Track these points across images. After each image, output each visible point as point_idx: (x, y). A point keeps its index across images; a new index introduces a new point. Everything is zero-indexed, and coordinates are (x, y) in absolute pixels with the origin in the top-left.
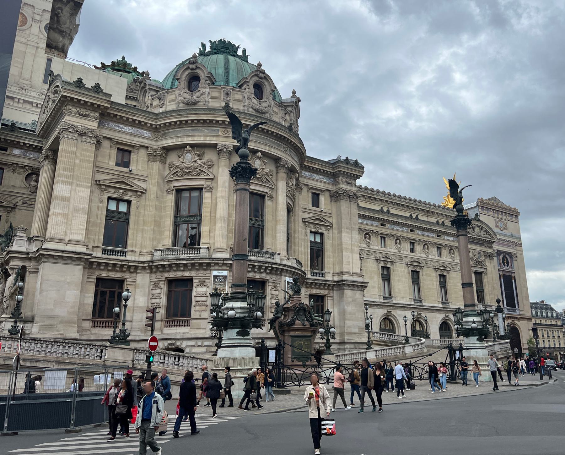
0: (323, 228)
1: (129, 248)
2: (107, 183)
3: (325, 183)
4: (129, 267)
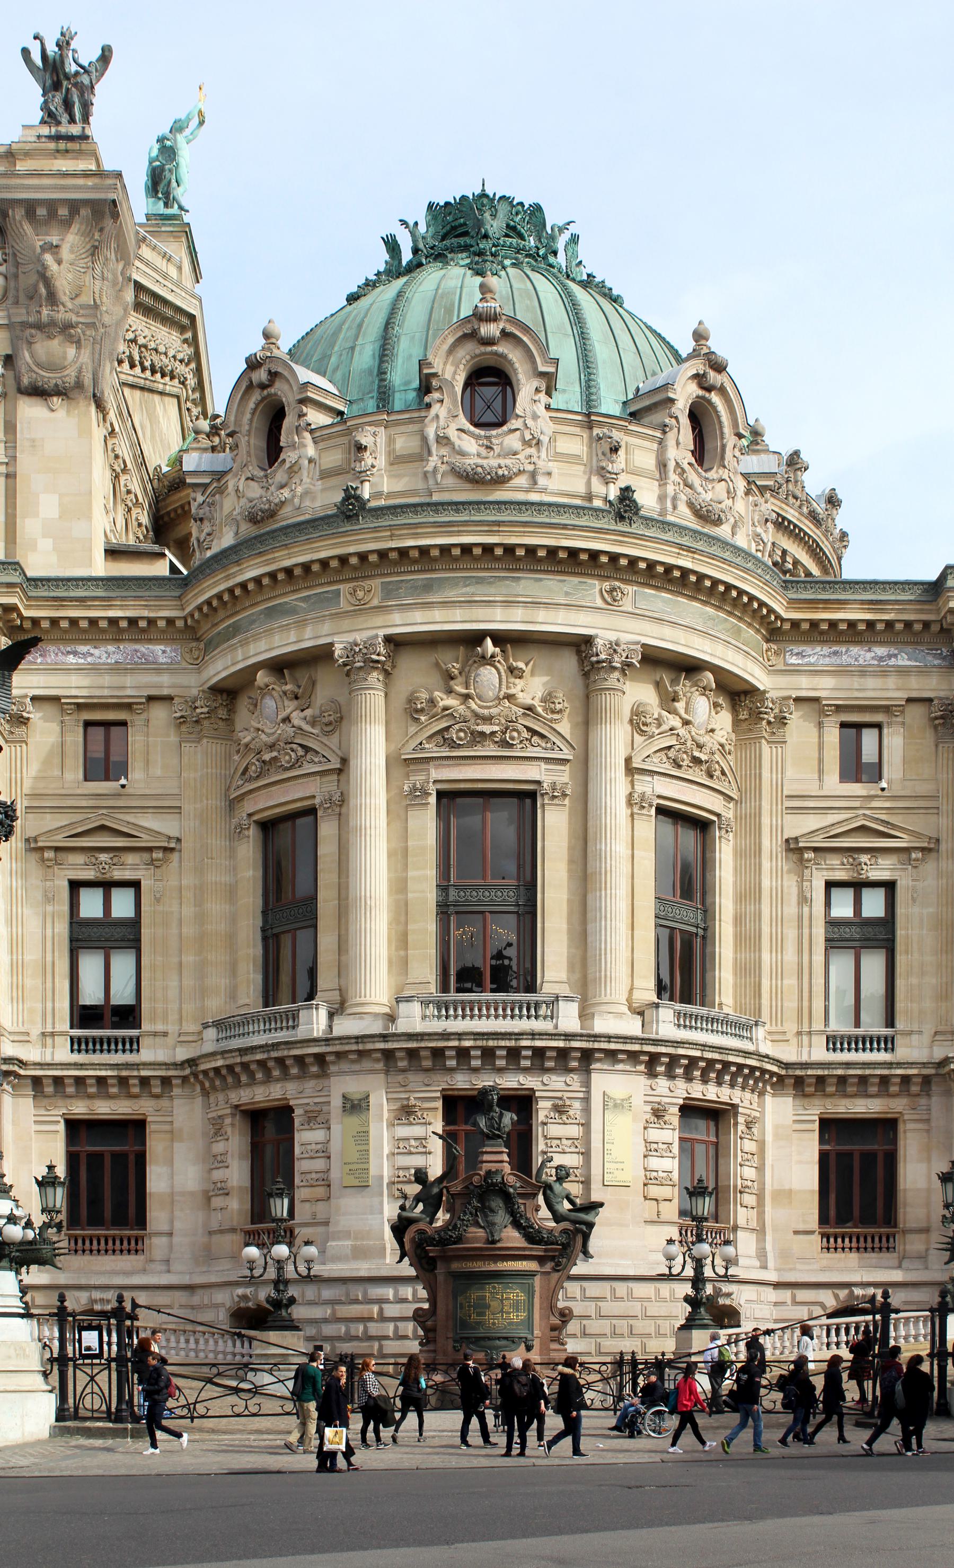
4: (145, 1082)
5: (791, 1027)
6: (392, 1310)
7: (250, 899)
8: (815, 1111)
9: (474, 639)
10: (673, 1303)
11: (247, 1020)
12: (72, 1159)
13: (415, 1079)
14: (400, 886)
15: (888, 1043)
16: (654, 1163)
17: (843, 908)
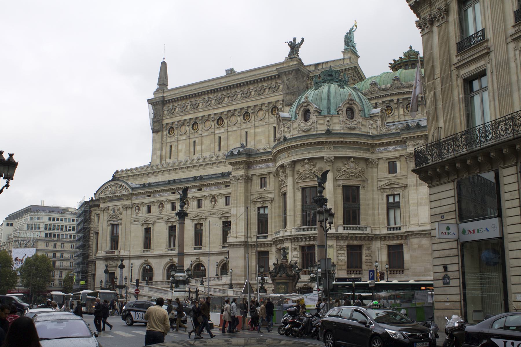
0: (398, 189)
1: (269, 233)
2: (255, 200)
3: (399, 150)
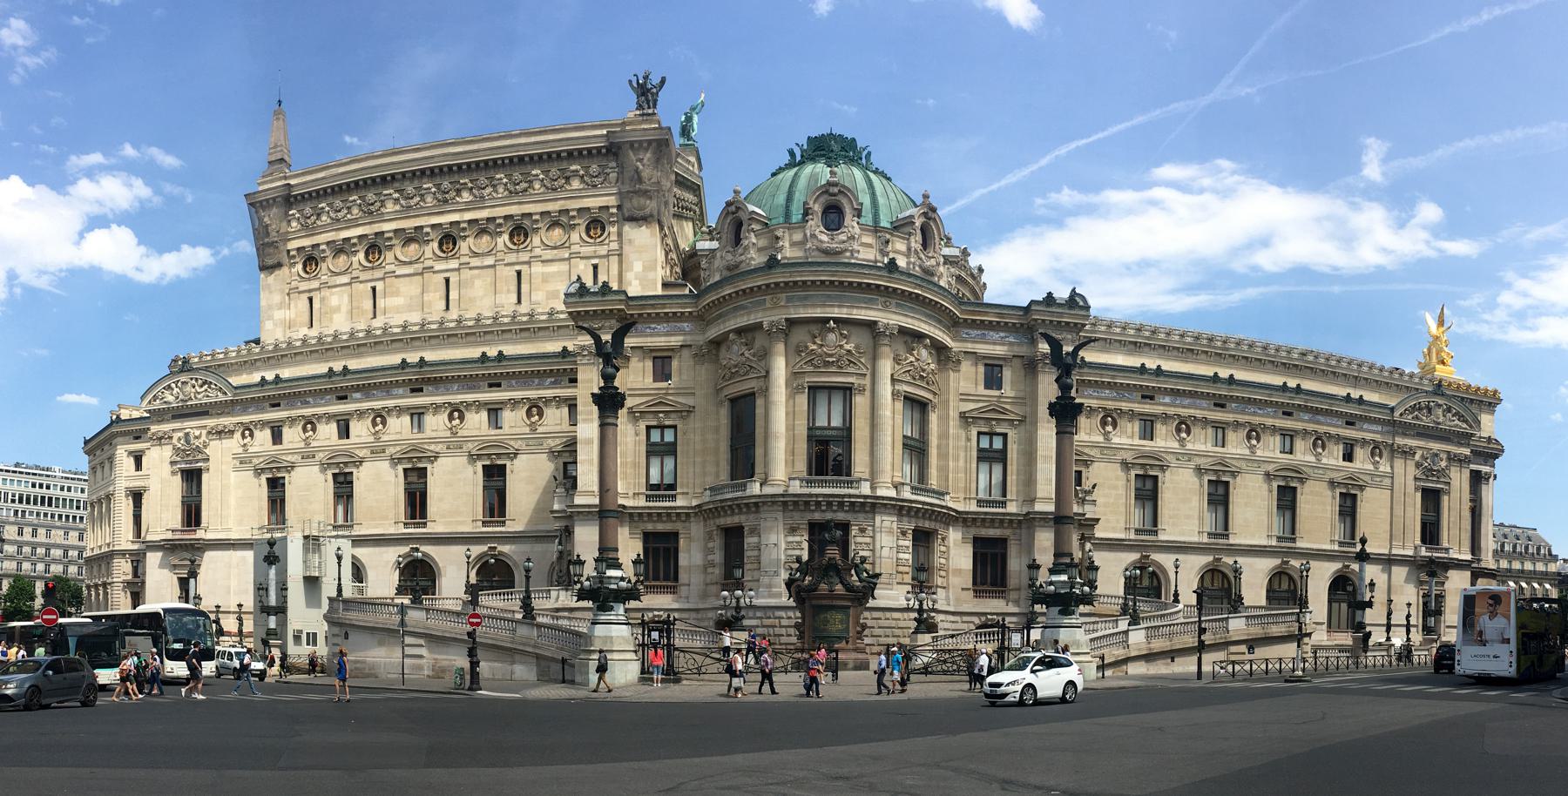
2: (642, 408)
4: (678, 514)
5: (962, 496)
6: (784, 622)
7: (725, 432)
8: (973, 532)
9: (827, 320)
10: (909, 621)
11: (724, 487)
12: (646, 550)
13: (797, 515)
14: (791, 428)
15: (1003, 504)
16: (901, 556)
17: (985, 443)
